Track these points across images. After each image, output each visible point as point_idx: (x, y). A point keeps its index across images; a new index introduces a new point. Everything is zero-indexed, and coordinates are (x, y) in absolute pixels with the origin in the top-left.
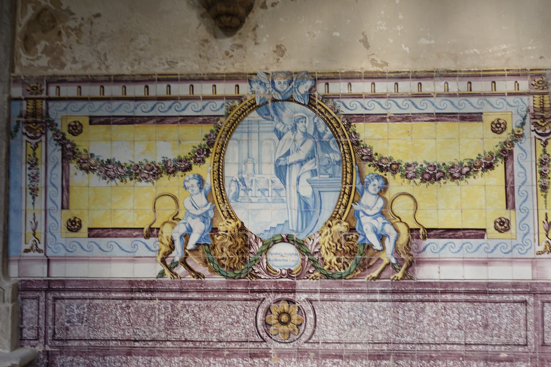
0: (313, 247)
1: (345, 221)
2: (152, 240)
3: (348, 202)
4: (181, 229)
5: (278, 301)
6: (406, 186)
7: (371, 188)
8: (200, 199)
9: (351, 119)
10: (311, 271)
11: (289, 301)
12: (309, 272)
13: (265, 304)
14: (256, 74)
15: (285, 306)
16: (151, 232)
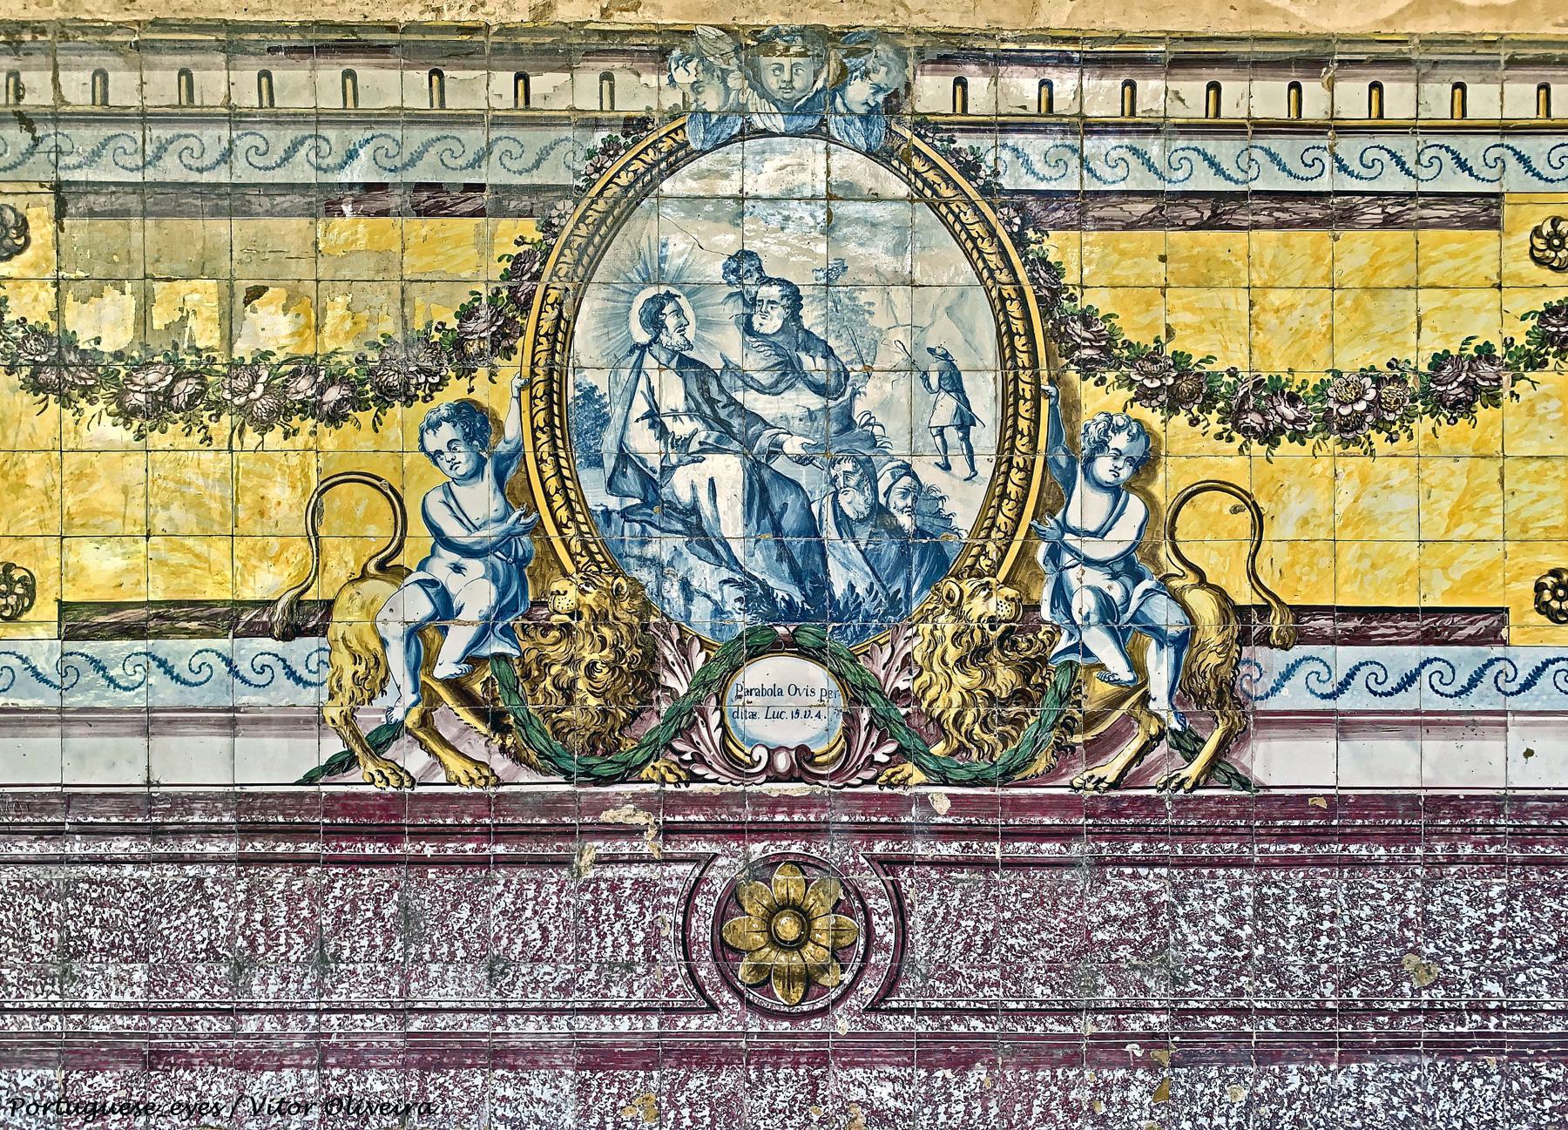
0: (894, 674)
1: (1007, 582)
2: (304, 646)
3: (1020, 515)
4: (420, 606)
5: (771, 863)
6: (1232, 461)
7: (1103, 467)
8: (481, 499)
9: (1034, 210)
10: (880, 757)
11: (800, 864)
12: (871, 761)
13: (718, 880)
14: (690, 34)
15: (786, 883)
16: (305, 618)
